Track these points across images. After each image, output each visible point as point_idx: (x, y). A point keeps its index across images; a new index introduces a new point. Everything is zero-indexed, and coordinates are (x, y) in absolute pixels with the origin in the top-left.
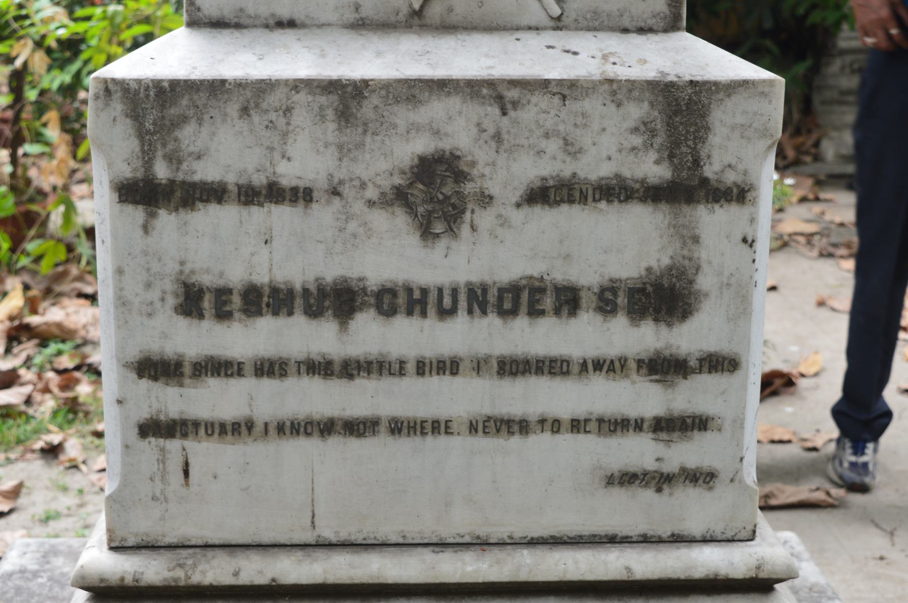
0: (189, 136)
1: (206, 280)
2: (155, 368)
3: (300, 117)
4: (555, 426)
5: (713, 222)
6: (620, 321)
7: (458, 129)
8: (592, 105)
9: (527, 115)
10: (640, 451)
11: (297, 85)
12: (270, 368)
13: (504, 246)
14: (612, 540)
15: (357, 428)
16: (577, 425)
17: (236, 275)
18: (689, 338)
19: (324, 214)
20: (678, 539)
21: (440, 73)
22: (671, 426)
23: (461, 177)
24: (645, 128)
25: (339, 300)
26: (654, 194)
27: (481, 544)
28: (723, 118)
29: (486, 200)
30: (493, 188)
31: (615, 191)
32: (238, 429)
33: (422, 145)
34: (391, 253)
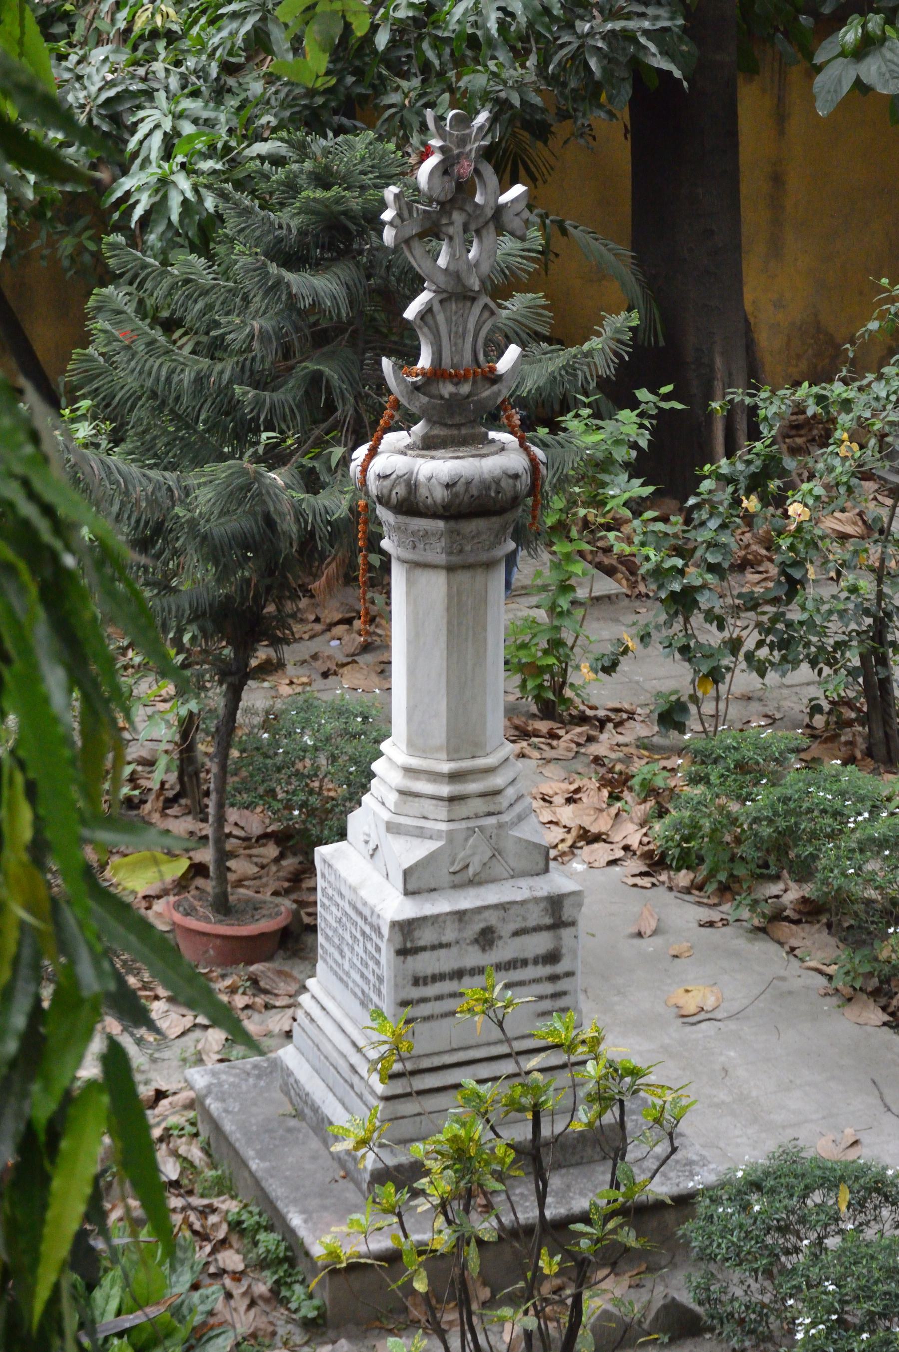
0: (416, 934)
1: (421, 975)
2: (404, 1004)
3: (448, 923)
5: (566, 933)
6: (540, 967)
7: (492, 919)
8: (531, 906)
9: (512, 912)
11: (447, 914)
12: (439, 998)
13: (505, 951)
17: (429, 972)
18: (559, 969)
19: (454, 950)
21: (486, 903)
22: (556, 996)
23: (493, 932)
24: (546, 910)
26: (549, 928)
28: (567, 903)
29: (500, 938)
30: (503, 934)
31: (537, 929)
32: (427, 1019)
33: (482, 925)
34: (474, 957)
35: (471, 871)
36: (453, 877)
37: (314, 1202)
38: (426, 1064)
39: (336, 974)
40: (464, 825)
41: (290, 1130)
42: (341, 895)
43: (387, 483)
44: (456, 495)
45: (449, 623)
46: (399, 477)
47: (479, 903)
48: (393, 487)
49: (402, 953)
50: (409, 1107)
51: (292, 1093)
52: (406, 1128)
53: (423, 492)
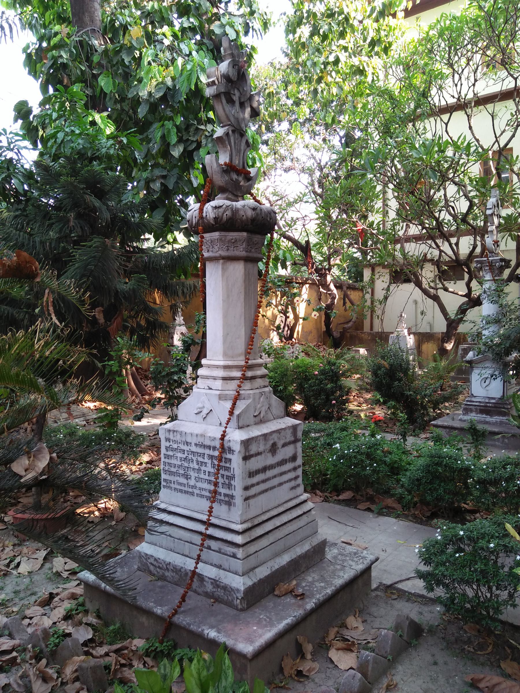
0: (250, 447)
4: (285, 482)
8: (287, 431)
10: (293, 484)
12: (258, 484)
14: (291, 499)
15: (266, 491)
16: (287, 482)
19: (263, 455)
20: (297, 496)
25: (264, 469)
27: (279, 506)
33: (272, 442)
34: (271, 460)
35: (262, 415)
36: (255, 419)
37: (212, 620)
38: (256, 522)
39: (181, 491)
40: (257, 391)
41: (161, 587)
42: (187, 443)
43: (221, 210)
44: (257, 214)
45: (245, 288)
46: (227, 206)
47: (270, 430)
48: (225, 211)
49: (246, 458)
50: (252, 548)
51: (152, 568)
52: (252, 561)
53: (242, 213)
